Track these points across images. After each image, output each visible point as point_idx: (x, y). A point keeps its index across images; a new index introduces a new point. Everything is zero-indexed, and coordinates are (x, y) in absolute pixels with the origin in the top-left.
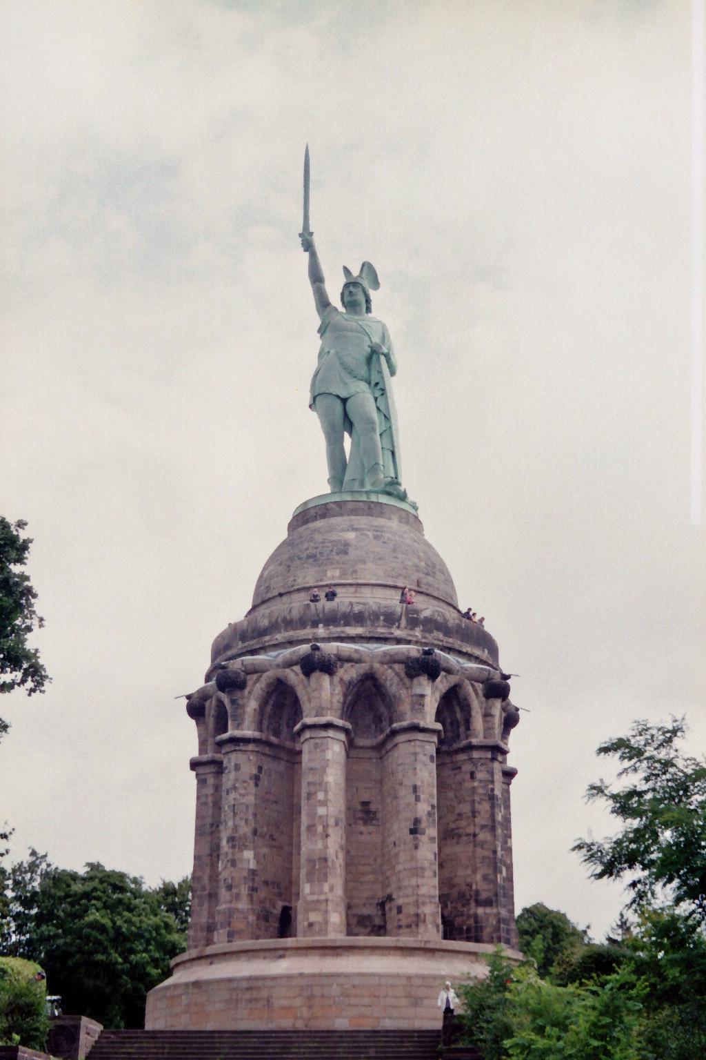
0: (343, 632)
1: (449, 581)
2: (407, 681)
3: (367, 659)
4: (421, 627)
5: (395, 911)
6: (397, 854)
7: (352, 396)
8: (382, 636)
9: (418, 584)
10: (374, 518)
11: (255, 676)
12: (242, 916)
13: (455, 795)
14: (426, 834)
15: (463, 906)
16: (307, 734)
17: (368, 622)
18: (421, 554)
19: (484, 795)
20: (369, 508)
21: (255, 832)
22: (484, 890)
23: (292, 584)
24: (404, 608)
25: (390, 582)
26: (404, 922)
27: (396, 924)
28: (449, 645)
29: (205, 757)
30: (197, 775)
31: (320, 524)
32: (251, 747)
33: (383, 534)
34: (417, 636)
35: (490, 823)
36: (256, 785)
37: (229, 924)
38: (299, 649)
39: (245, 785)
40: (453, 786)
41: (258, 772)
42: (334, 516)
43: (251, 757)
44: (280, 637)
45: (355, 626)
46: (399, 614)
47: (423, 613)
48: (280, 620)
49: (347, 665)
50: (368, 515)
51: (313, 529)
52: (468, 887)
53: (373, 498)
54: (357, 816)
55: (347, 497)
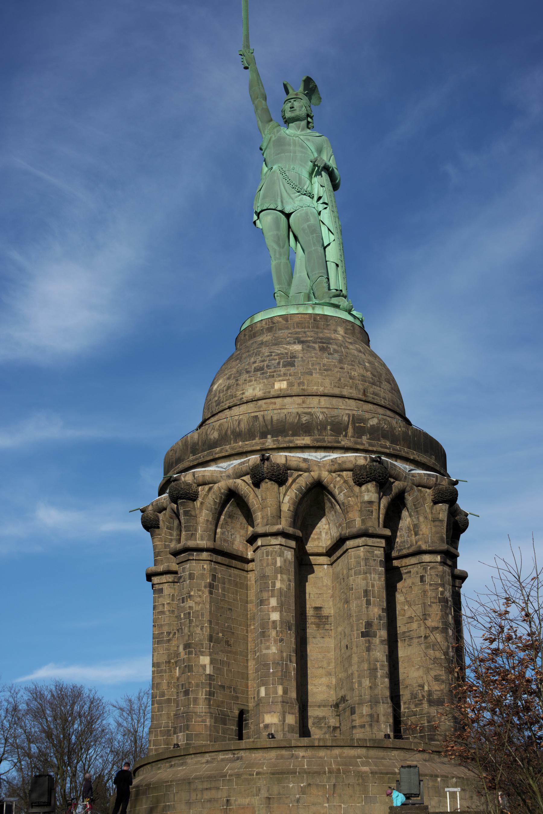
0: (291, 442)
1: (396, 390)
2: (357, 489)
3: (316, 468)
4: (368, 436)
5: (348, 713)
6: (350, 657)
8: (329, 445)
9: (364, 393)
10: (320, 330)
11: (207, 487)
12: (200, 719)
13: (406, 598)
14: (378, 637)
15: (416, 706)
16: (259, 542)
18: (367, 364)
19: (435, 598)
20: (315, 320)
21: (211, 639)
22: (436, 691)
23: (241, 397)
24: (351, 419)
25: (337, 391)
26: (357, 723)
27: (349, 725)
28: (397, 453)
29: (161, 568)
30: (153, 585)
31: (267, 337)
32: (205, 555)
33: (330, 346)
34: (364, 444)
35: (440, 625)
36: (211, 593)
37: (187, 727)
38: (249, 460)
39: (200, 593)
40: (404, 590)
41: (213, 580)
42: (280, 329)
43: (205, 566)
44: (228, 449)
45: (303, 436)
46: (346, 423)
47: (369, 422)
48: (229, 432)
49: (296, 474)
50: (313, 327)
51: (261, 342)
52: (421, 688)
53: (319, 311)
55: (293, 311)
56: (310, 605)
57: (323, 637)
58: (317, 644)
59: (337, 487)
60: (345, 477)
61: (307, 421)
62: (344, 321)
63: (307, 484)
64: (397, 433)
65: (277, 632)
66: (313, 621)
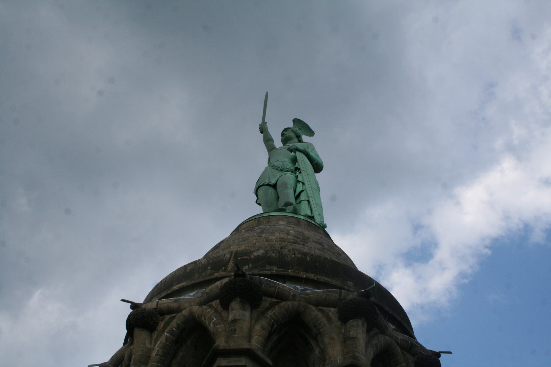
2: (224, 313)
4: (250, 265)
7: (278, 180)
17: (196, 275)
24: (233, 255)
49: (168, 317)
59: (207, 318)
60: (214, 305)
61: (191, 269)
62: (288, 217)
63: (178, 324)
64: (289, 259)
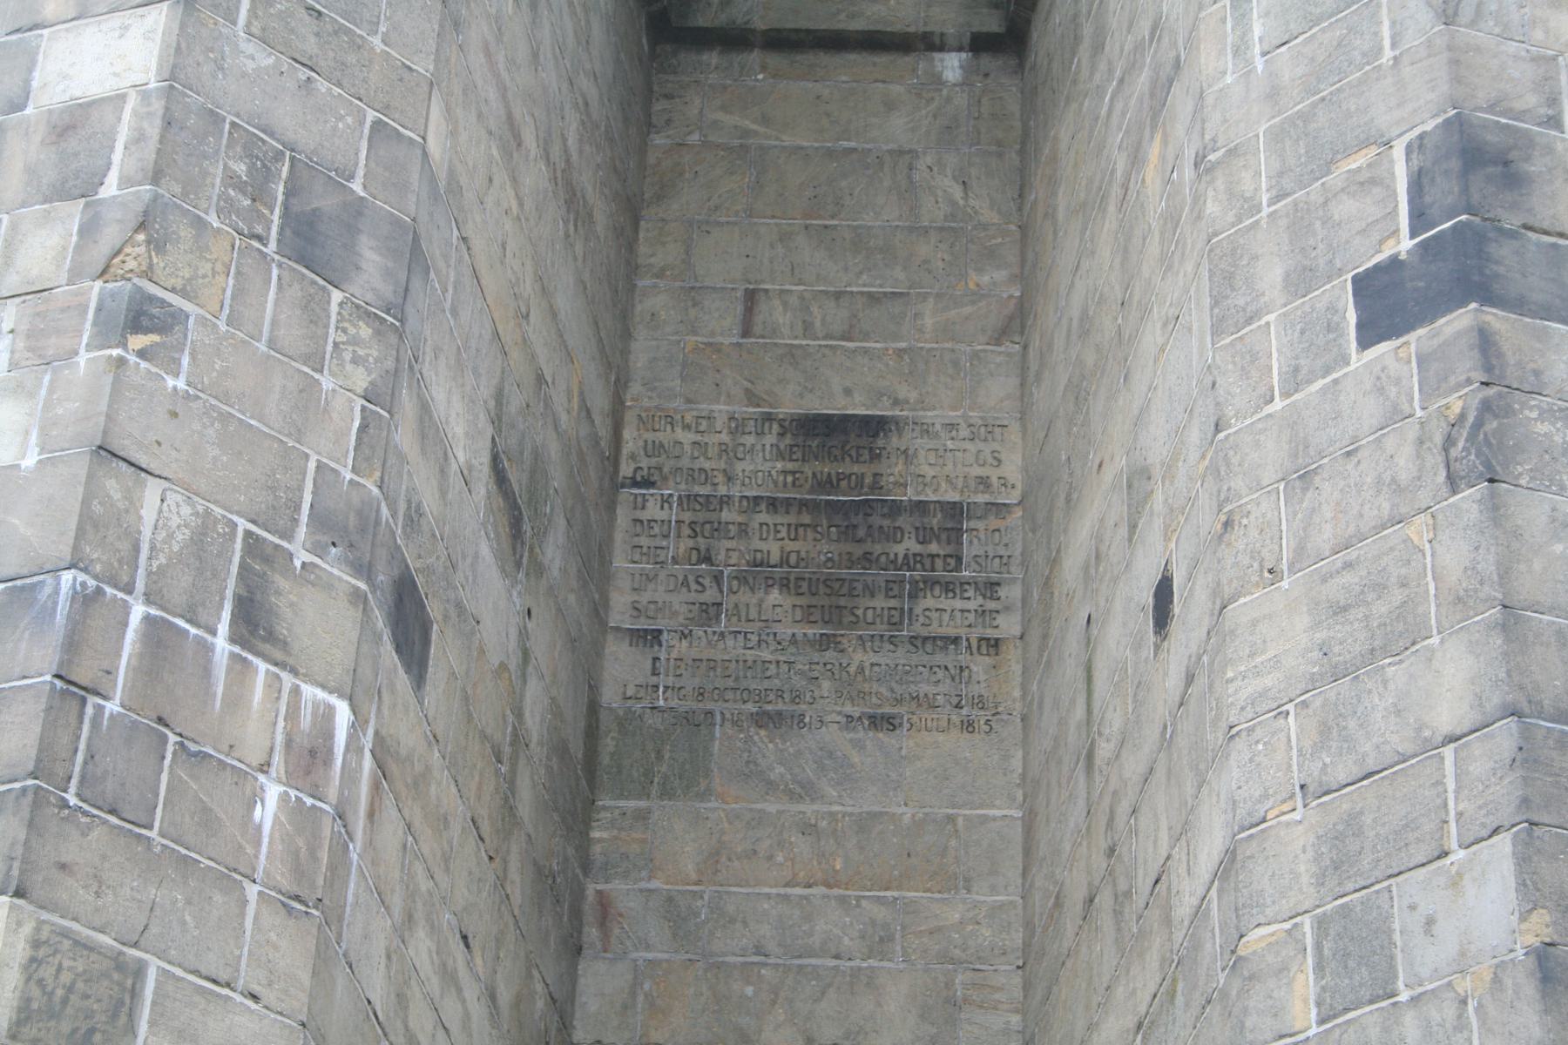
54: (731, 554)
56: (752, 398)
57: (883, 722)
58: (807, 791)
65: (88, 230)
66: (774, 549)
